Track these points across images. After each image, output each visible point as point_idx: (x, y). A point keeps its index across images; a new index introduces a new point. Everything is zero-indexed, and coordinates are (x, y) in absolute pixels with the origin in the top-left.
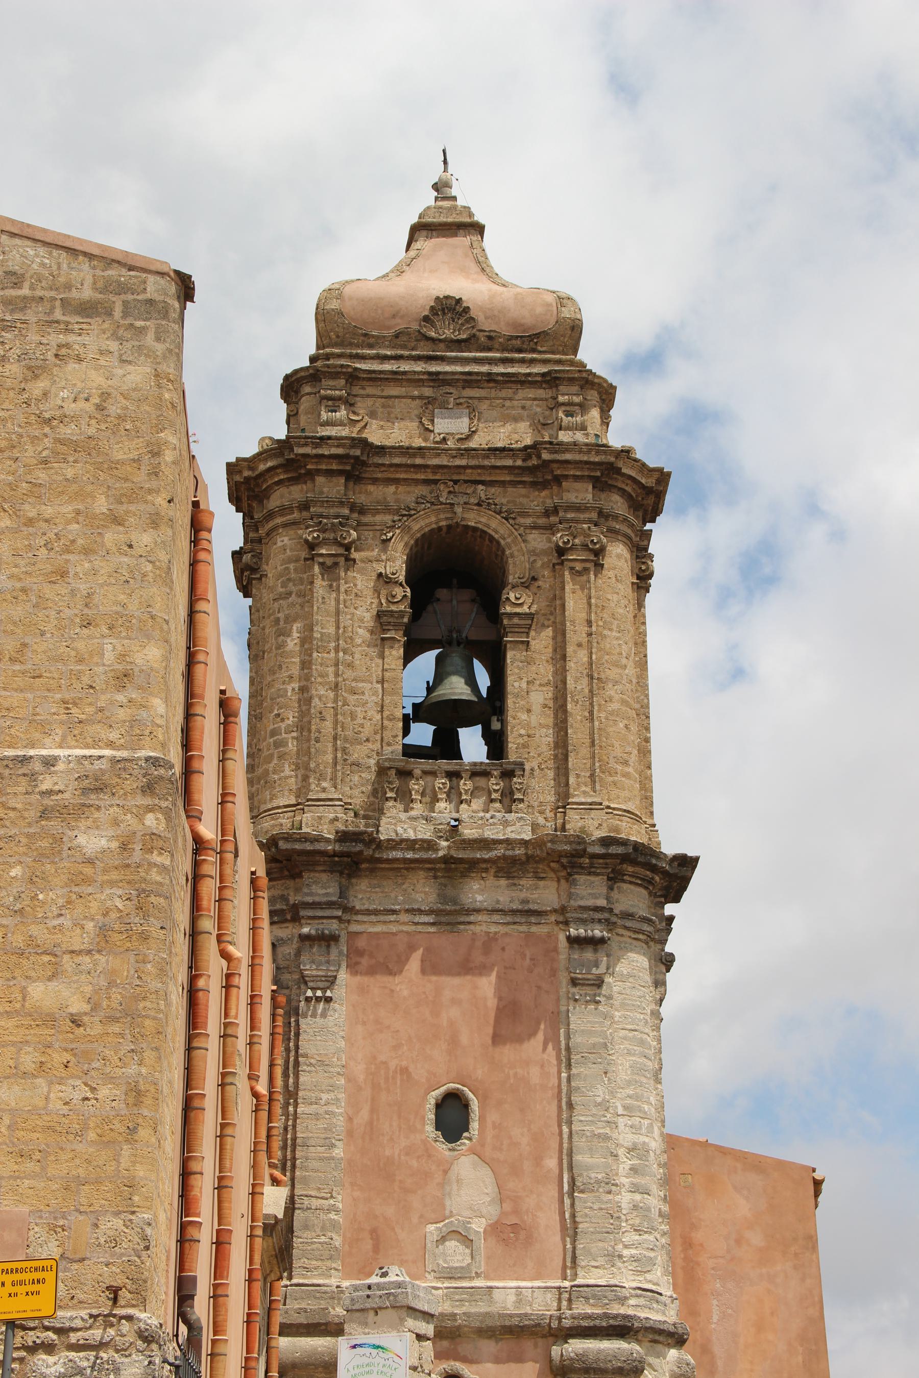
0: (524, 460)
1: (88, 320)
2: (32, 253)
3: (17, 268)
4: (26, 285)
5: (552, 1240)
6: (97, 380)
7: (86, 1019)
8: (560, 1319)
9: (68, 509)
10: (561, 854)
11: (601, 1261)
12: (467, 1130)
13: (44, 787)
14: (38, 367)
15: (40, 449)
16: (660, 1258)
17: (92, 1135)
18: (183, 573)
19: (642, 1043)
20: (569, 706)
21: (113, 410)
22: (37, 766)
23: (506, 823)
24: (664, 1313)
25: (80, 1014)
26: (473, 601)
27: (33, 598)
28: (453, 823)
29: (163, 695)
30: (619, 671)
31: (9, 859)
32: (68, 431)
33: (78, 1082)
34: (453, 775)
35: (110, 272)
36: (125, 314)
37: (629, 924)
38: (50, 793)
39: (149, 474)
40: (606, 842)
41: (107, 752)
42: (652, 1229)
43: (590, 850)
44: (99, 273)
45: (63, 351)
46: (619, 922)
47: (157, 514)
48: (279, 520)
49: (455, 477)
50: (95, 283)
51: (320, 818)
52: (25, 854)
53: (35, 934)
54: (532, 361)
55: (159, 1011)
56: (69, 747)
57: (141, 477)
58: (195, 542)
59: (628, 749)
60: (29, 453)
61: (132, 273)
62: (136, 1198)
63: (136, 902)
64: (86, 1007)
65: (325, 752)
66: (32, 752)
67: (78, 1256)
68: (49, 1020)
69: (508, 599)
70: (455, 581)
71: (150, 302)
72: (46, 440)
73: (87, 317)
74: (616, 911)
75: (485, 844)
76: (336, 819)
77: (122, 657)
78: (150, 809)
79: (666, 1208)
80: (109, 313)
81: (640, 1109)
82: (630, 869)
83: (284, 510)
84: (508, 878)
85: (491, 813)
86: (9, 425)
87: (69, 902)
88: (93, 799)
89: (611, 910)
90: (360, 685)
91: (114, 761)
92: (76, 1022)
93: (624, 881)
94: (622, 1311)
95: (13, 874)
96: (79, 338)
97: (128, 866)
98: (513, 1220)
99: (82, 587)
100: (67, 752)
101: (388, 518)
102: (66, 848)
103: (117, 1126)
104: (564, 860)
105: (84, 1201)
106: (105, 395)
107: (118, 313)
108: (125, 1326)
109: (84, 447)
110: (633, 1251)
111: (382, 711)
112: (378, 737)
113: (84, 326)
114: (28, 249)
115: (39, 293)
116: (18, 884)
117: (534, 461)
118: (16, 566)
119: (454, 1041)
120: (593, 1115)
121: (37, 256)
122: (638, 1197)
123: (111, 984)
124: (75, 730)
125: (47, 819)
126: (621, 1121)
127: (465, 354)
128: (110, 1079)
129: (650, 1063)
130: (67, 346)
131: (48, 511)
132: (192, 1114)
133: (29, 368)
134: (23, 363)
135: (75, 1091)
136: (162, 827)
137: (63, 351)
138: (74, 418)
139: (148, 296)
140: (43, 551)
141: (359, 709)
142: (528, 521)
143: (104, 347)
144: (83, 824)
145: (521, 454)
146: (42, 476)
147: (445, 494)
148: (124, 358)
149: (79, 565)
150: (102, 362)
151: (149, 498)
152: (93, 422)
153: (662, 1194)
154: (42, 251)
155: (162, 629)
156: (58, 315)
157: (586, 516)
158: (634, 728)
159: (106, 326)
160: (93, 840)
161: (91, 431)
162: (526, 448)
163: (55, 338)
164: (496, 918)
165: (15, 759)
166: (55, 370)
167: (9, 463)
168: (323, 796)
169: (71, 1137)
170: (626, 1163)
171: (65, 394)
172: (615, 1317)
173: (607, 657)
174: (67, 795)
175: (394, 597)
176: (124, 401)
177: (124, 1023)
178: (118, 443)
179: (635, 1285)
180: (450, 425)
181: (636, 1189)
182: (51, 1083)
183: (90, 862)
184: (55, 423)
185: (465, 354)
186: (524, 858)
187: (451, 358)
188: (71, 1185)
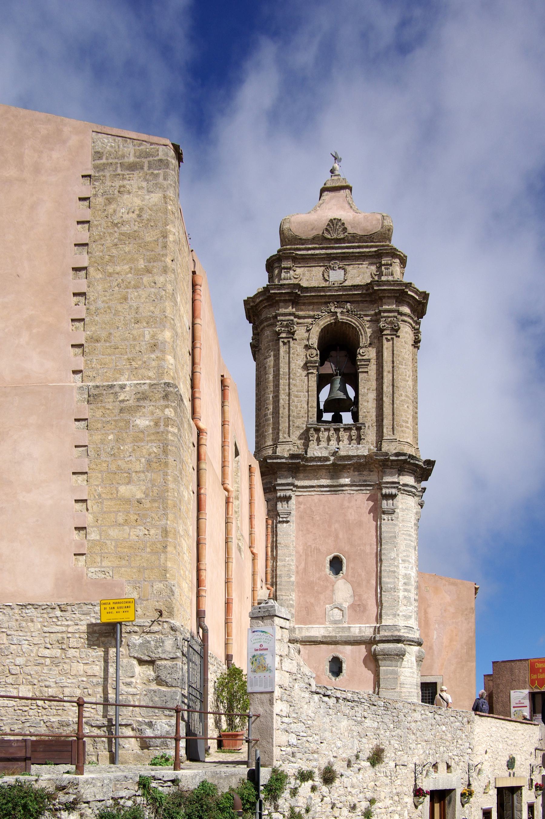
0: (366, 290)
1: (133, 172)
2: (106, 141)
3: (100, 149)
4: (104, 157)
5: (373, 610)
6: (137, 202)
7: (143, 501)
8: (375, 637)
9: (126, 267)
10: (380, 461)
11: (391, 617)
12: (342, 570)
13: (121, 398)
14: (111, 198)
15: (113, 239)
16: (414, 616)
17: (148, 550)
18: (186, 303)
19: (410, 535)
20: (384, 399)
21: (145, 216)
22: (117, 389)
23: (357, 449)
24: (414, 635)
25: (141, 499)
26: (346, 356)
27: (113, 311)
28: (337, 450)
29: (172, 354)
30: (405, 383)
31: (108, 432)
32: (125, 229)
33: (142, 528)
34: (337, 430)
35: (142, 147)
36: (150, 168)
37: (406, 488)
38: (123, 401)
39: (162, 247)
40: (398, 454)
41: (148, 381)
42: (411, 604)
43: (391, 458)
44: (137, 148)
45: (122, 189)
46: (402, 488)
47: (166, 266)
49: (338, 300)
50: (135, 153)
51: (283, 449)
52: (114, 429)
53: (120, 464)
54: (371, 247)
55: (175, 497)
56: (132, 380)
57: (159, 250)
58: (194, 291)
59: (408, 416)
60: (109, 242)
61: (152, 147)
62: (168, 575)
63: (162, 449)
64: (143, 496)
65: (285, 422)
66: (115, 383)
67: (145, 598)
68: (128, 501)
69: (359, 353)
70: (338, 347)
71: (161, 160)
72: (116, 234)
73: (132, 171)
74: (401, 483)
75: (349, 458)
76: (290, 450)
77: (153, 336)
78: (167, 407)
79: (417, 597)
80: (142, 168)
81: (408, 561)
82: (407, 466)
84: (358, 471)
85: (352, 445)
86: (99, 228)
87: (134, 450)
88: (142, 403)
89: (399, 483)
90: (299, 393)
91: (151, 385)
92: (139, 502)
93: (405, 471)
94: (398, 634)
95: (109, 438)
96: (129, 182)
97: (158, 433)
98: (358, 603)
99: (134, 304)
100: (130, 382)
102: (131, 426)
103: (159, 546)
104: (381, 463)
105: (146, 576)
107: (146, 168)
108: (166, 625)
109: (133, 236)
110: (404, 613)
111: (308, 404)
112: (307, 415)
113: (131, 176)
114: (105, 139)
115: (110, 161)
116: (112, 442)
118: (105, 296)
119: (337, 537)
120: (390, 564)
121: (109, 142)
122: (406, 594)
123: (153, 485)
124: (134, 371)
125: (123, 413)
126: (401, 566)
127: (343, 245)
128: (154, 526)
129: (412, 543)
130: (124, 186)
131: (118, 269)
132: (200, 546)
133: (107, 199)
134: (104, 197)
135: (140, 531)
136: (173, 414)
137: (122, 189)
138: (128, 222)
139: (159, 157)
140: (117, 288)
141: (299, 404)
143: (140, 185)
144: (138, 414)
145: (365, 288)
146: (114, 252)
147: (333, 308)
148: (149, 190)
149: (133, 294)
150: (140, 193)
151: (163, 259)
152: (136, 223)
153: (416, 593)
154: (111, 138)
155: (171, 323)
156: (119, 171)
158: (411, 407)
159: (141, 174)
160: (142, 422)
161: (136, 228)
162: (368, 284)
163: (118, 183)
165: (108, 386)
166: (119, 199)
167: (100, 246)
168: (285, 440)
169: (140, 551)
170: (402, 581)
171: (123, 210)
172: (396, 636)
173: (400, 377)
174: (131, 402)
175: (312, 355)
176: (150, 212)
177: (159, 502)
178: (148, 233)
179: (403, 625)
180: (336, 276)
181: (405, 590)
182: (130, 528)
183: (142, 432)
184: (119, 225)
185: (343, 245)
186: (364, 463)
187: (336, 247)
188: (141, 570)
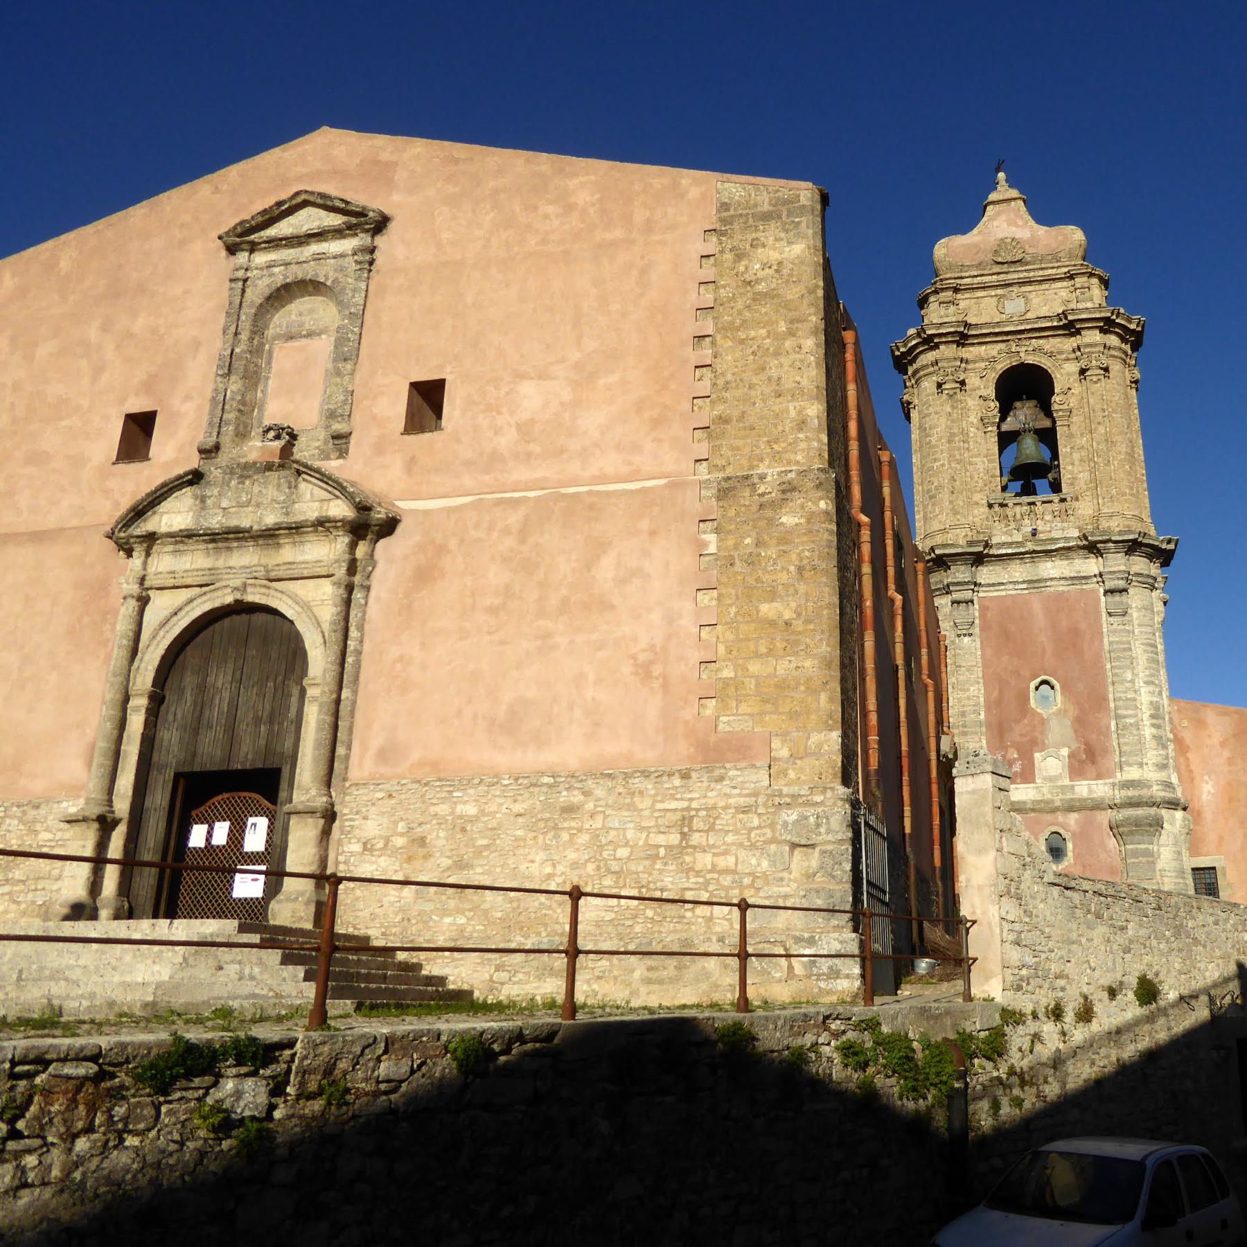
6: (774, 256)
9: (763, 332)
21: (785, 271)
22: (756, 480)
32: (761, 287)
36: (788, 216)
48: (922, 373)
60: (740, 305)
64: (794, 616)
68: (773, 623)
77: (800, 412)
80: (780, 217)
83: (924, 367)
91: (800, 473)
101: (983, 365)
106: (780, 263)
109: (770, 295)
117: (1064, 321)
124: (776, 457)
131: (753, 333)
140: (751, 357)
142: (1064, 356)
157: (1097, 349)
163: (750, 236)
164: (1062, 582)
